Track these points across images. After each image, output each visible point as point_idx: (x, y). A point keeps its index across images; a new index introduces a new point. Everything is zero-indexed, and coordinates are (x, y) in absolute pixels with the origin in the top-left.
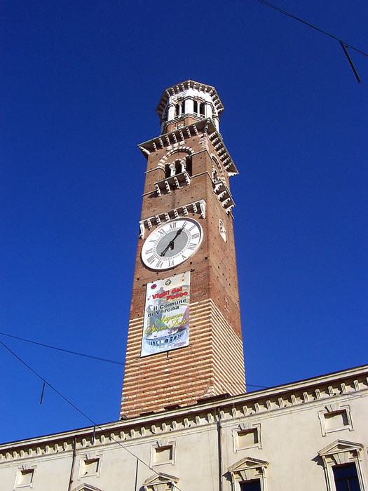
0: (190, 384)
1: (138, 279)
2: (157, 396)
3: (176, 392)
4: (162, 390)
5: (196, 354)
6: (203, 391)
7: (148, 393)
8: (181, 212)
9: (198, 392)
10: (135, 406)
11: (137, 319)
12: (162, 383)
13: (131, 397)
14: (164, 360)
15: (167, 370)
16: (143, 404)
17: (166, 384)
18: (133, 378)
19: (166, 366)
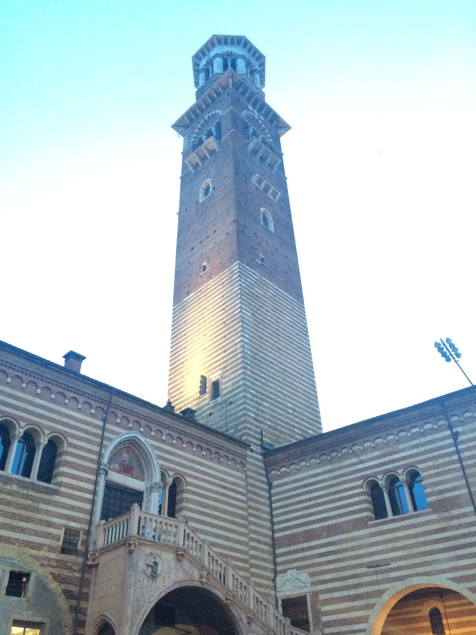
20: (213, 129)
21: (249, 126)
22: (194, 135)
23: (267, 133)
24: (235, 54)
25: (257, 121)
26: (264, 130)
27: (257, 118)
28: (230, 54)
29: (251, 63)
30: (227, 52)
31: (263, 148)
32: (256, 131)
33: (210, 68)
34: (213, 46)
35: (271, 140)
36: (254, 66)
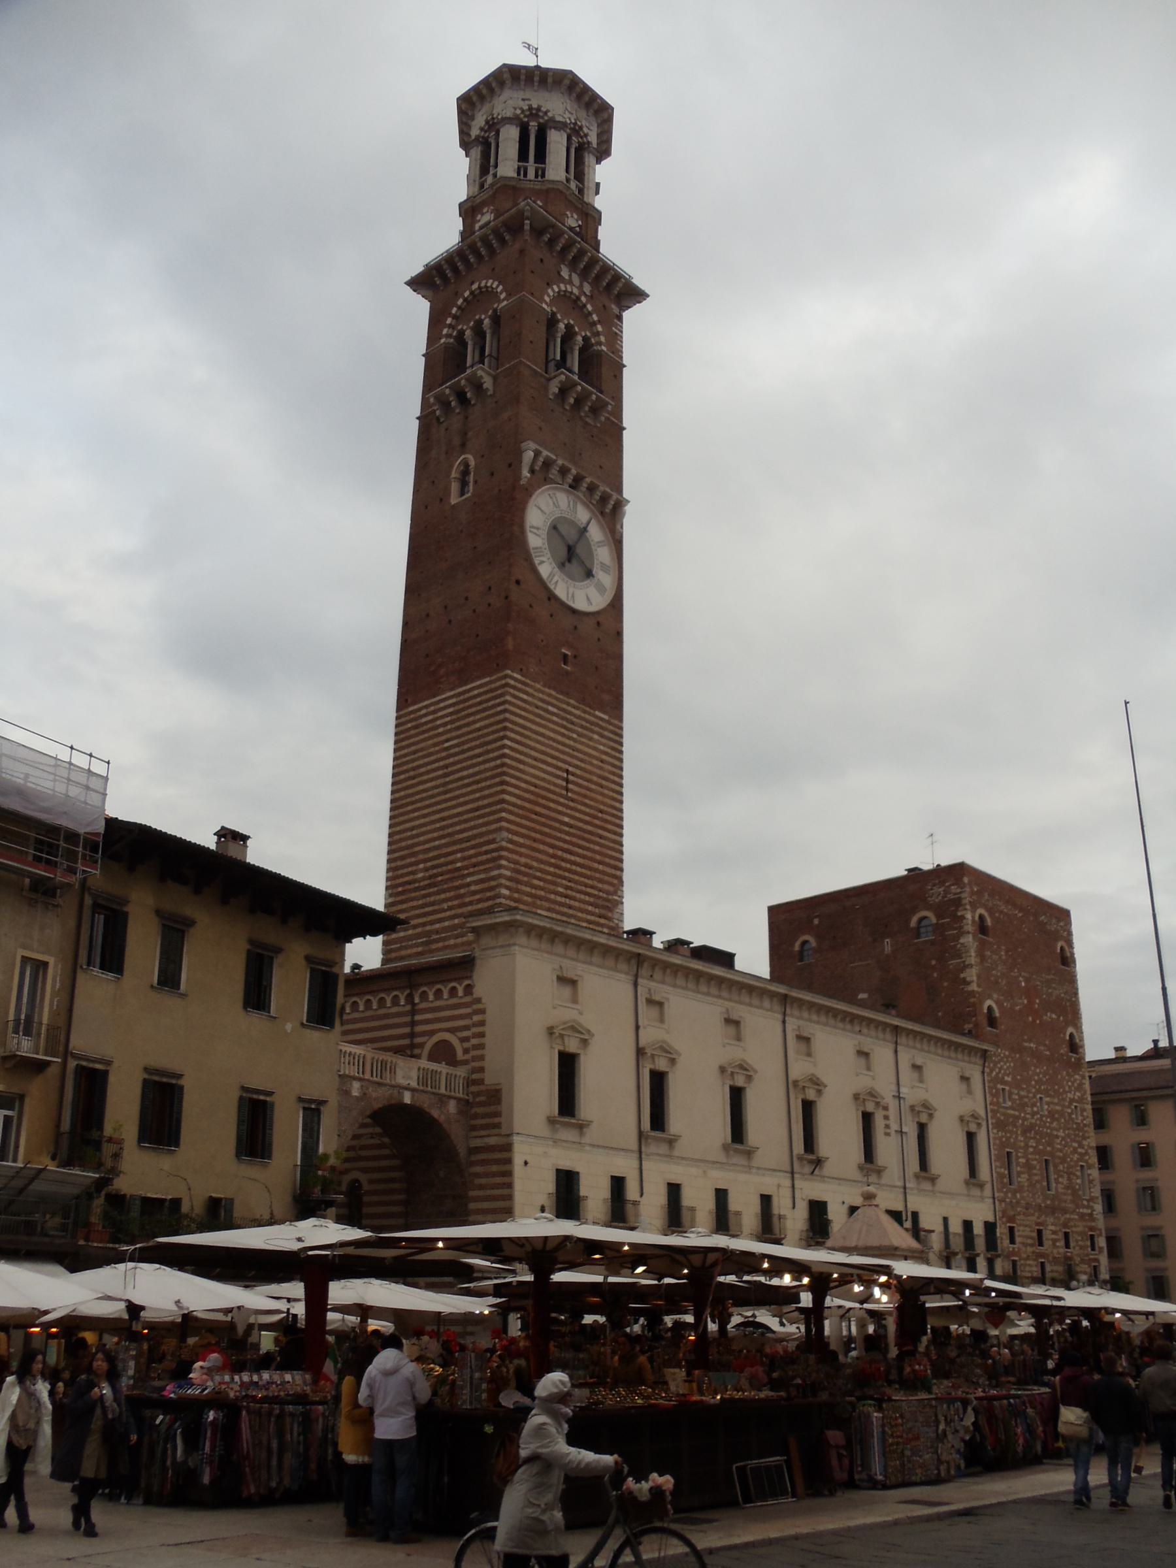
0: (596, 865)
1: (518, 582)
2: (553, 861)
3: (579, 869)
4: (560, 853)
5: (605, 816)
6: (611, 889)
7: (541, 847)
8: (592, 489)
9: (606, 887)
10: (523, 860)
11: (519, 677)
12: (560, 839)
13: (515, 838)
14: (561, 796)
15: (566, 819)
16: (535, 864)
17: (566, 846)
18: (519, 802)
19: (564, 810)
20: (487, 322)
21: (558, 321)
22: (449, 321)
23: (594, 324)
24: (546, 113)
25: (578, 298)
26: (590, 314)
27: (576, 291)
28: (534, 113)
29: (581, 128)
30: (531, 108)
31: (579, 388)
32: (572, 326)
33: (492, 141)
34: (502, 84)
35: (603, 339)
36: (586, 135)
